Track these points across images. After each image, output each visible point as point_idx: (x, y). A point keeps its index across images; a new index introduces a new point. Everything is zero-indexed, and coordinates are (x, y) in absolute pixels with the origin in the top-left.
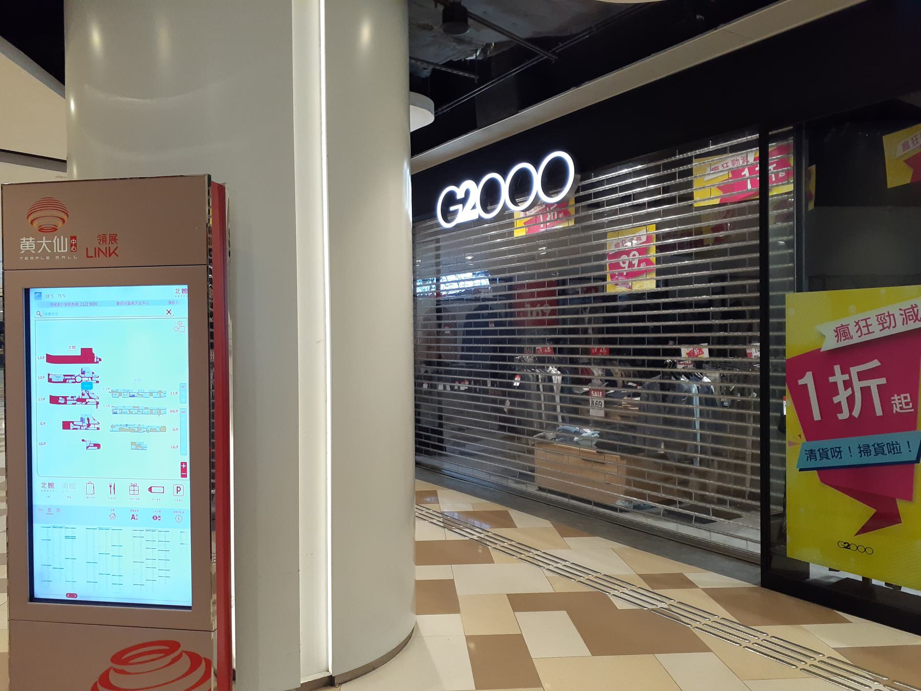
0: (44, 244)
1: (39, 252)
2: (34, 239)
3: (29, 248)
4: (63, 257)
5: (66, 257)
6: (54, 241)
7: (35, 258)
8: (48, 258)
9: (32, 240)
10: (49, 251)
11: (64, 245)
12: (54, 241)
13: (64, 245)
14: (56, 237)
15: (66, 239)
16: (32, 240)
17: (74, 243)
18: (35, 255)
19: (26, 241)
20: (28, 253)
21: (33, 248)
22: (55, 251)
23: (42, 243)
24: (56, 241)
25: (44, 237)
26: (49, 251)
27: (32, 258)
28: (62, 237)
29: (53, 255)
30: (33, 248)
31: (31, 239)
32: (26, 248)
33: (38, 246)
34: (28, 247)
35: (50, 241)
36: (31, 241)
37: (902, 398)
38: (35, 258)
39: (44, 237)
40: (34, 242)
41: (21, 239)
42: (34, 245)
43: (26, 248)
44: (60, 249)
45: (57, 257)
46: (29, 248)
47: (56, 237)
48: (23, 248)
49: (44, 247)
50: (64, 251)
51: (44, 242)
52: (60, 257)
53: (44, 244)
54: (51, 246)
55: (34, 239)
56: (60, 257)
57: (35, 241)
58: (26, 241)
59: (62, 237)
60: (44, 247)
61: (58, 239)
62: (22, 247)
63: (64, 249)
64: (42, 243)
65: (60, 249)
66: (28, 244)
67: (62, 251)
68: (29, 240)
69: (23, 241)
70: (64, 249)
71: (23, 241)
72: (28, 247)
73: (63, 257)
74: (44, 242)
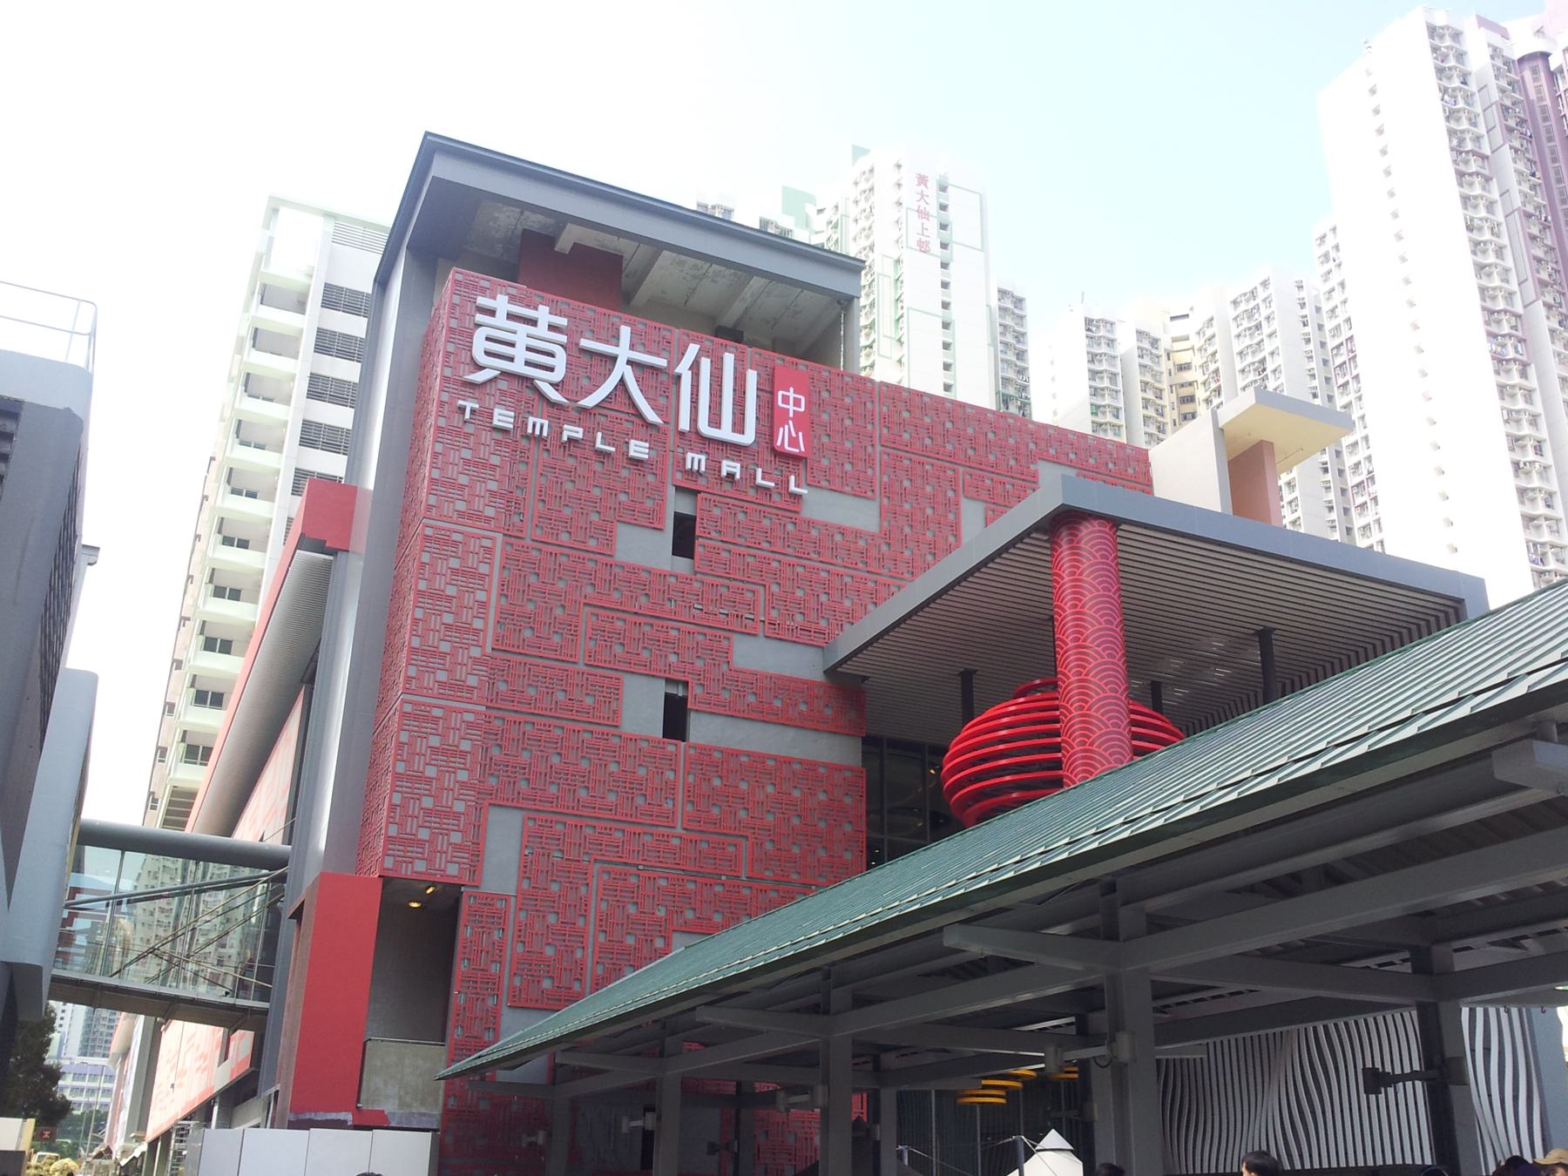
0: (621, 369)
1: (590, 401)
2: (562, 321)
3: (528, 363)
6: (683, 368)
9: (552, 328)
10: (652, 416)
11: (739, 403)
12: (683, 368)
13: (739, 403)
14: (693, 349)
15: (752, 377)
16: (552, 328)
17: (791, 408)
19: (511, 317)
21: (551, 369)
22: (684, 425)
23: (614, 359)
24: (695, 368)
25: (625, 332)
30: (551, 369)
32: (511, 359)
34: (520, 354)
39: (625, 332)
40: (563, 339)
41: (482, 301)
42: (561, 355)
43: (511, 359)
44: (715, 421)
45: (696, 460)
46: (528, 363)
48: (488, 353)
49: (622, 381)
51: (623, 351)
54: (660, 382)
55: (562, 321)
58: (511, 317)
60: (622, 381)
61: (706, 364)
63: (739, 426)
64: (614, 359)
65: (715, 421)
67: (726, 433)
69: (491, 312)
70: (739, 426)
71: (491, 312)
72: (520, 354)
73: (729, 466)
74: (623, 351)
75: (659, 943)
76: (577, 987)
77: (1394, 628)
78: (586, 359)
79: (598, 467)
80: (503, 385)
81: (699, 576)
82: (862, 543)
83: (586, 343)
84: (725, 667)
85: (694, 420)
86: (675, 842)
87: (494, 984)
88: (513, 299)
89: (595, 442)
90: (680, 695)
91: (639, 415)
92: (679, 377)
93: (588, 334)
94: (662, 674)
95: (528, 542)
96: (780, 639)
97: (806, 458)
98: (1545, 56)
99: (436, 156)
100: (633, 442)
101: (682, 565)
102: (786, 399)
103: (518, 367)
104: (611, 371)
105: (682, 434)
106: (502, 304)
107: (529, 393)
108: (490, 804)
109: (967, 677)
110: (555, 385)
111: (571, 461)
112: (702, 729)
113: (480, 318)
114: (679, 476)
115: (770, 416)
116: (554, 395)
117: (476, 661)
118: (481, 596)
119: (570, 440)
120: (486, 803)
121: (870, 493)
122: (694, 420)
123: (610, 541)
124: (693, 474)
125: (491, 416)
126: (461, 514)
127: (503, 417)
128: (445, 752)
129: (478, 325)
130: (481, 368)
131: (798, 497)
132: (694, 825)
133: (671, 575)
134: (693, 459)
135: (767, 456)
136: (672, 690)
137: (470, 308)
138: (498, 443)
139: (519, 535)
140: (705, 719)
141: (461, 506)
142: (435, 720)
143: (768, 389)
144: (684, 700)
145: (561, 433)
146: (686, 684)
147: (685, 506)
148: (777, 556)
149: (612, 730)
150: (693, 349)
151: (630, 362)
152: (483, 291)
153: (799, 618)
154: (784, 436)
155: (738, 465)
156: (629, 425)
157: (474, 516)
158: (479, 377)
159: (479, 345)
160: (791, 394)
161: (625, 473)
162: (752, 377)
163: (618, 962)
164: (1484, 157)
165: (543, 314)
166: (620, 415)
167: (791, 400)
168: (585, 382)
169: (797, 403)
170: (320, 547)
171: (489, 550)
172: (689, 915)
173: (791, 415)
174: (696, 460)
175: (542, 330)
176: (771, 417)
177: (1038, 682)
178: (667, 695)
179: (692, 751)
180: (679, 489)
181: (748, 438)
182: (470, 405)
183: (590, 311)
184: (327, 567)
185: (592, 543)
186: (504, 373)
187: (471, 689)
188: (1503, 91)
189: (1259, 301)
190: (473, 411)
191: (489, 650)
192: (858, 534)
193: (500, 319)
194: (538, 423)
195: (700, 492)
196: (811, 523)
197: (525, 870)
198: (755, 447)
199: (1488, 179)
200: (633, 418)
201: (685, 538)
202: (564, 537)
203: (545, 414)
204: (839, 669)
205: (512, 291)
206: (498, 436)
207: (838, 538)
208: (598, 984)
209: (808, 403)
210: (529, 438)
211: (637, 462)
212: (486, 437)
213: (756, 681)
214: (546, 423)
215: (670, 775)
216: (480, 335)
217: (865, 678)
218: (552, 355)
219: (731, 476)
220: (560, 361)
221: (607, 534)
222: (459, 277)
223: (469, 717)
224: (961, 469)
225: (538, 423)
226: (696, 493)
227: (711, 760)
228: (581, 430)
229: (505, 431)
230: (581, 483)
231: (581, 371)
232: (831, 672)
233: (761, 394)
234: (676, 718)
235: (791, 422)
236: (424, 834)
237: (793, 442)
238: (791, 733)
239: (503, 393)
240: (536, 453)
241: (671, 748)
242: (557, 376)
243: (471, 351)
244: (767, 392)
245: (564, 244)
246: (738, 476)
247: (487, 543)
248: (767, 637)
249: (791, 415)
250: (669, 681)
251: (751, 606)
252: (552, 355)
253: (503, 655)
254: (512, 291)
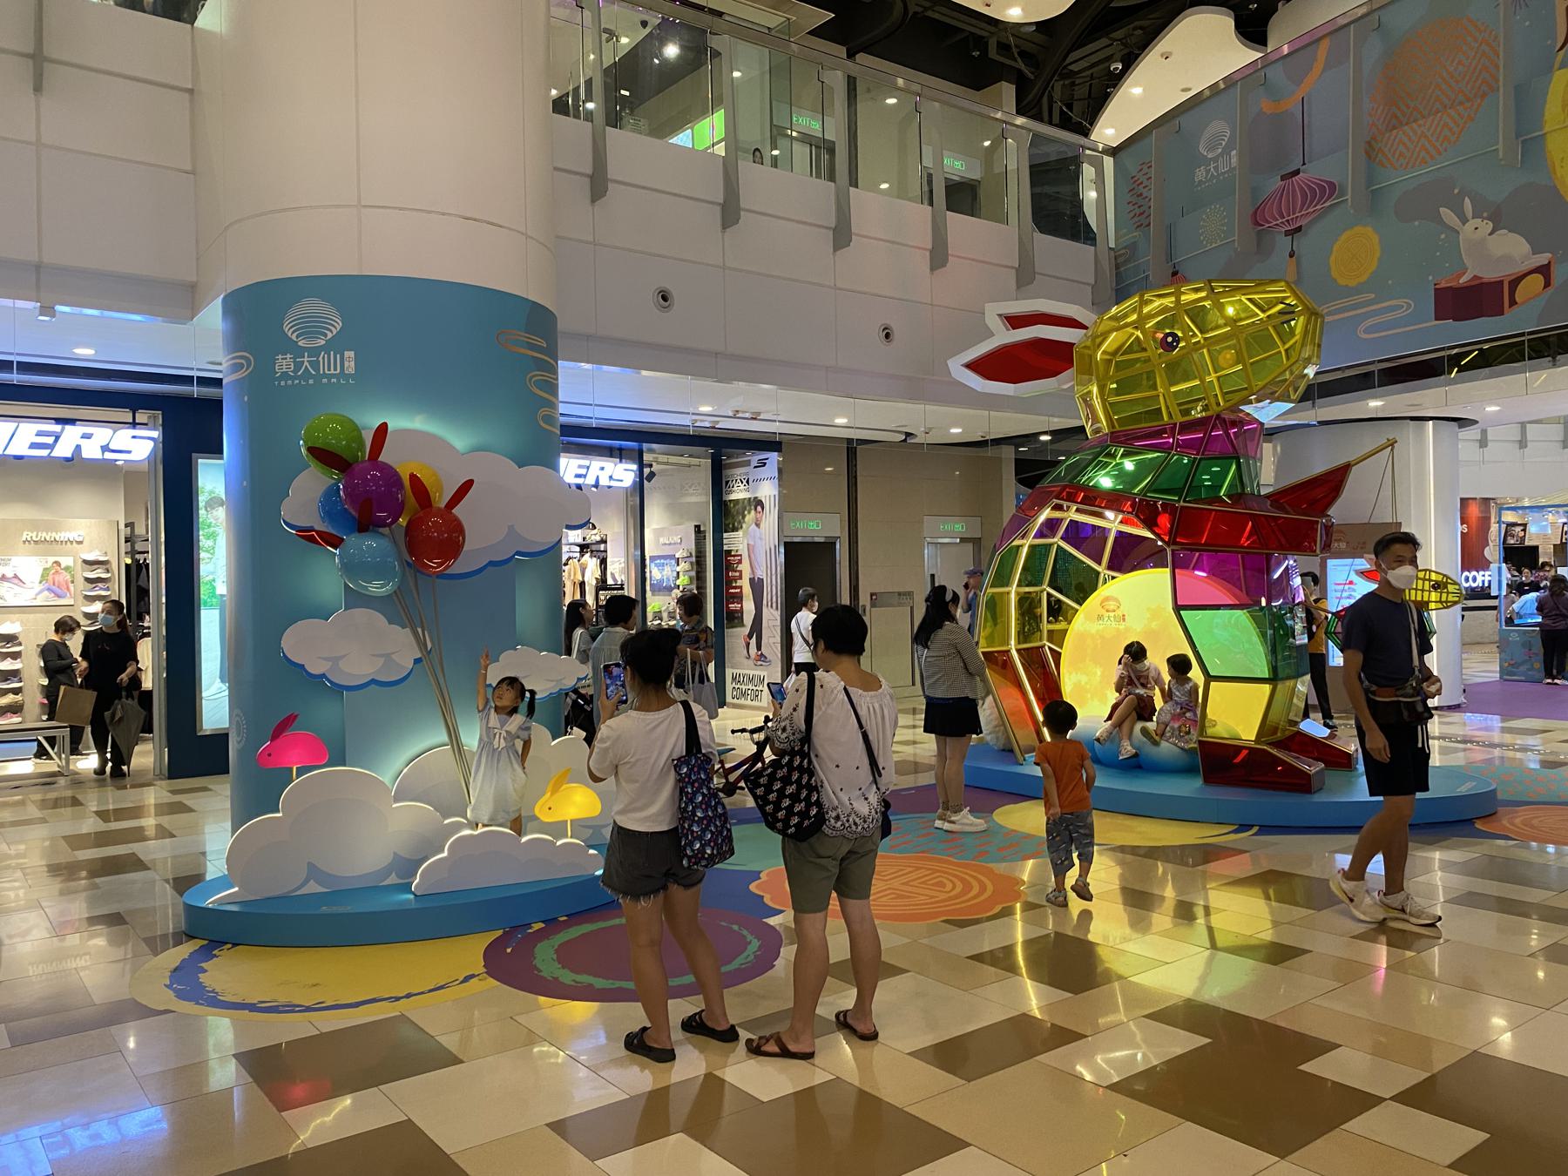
0: (306, 363)
4: (334, 380)
5: (339, 381)
6: (321, 359)
7: (293, 382)
8: (311, 382)
10: (314, 373)
14: (323, 353)
15: (338, 356)
18: (293, 378)
19: (282, 359)
20: (285, 375)
22: (321, 372)
24: (323, 358)
25: (306, 354)
26: (314, 373)
27: (290, 382)
28: (332, 353)
29: (318, 377)
31: (288, 356)
33: (298, 366)
36: (288, 360)
37: (1486, 575)
38: (293, 382)
39: (306, 354)
44: (329, 370)
45: (325, 381)
47: (323, 353)
49: (306, 366)
51: (306, 359)
52: (329, 380)
53: (306, 363)
54: (315, 365)
56: (329, 380)
57: (294, 358)
58: (282, 359)
59: (332, 353)
60: (306, 366)
62: (277, 368)
63: (335, 370)
65: (329, 370)
66: (284, 364)
67: (332, 372)
68: (286, 359)
72: (284, 367)
73: (334, 380)
122: (324, 369)
165: (288, 356)
220: (292, 367)
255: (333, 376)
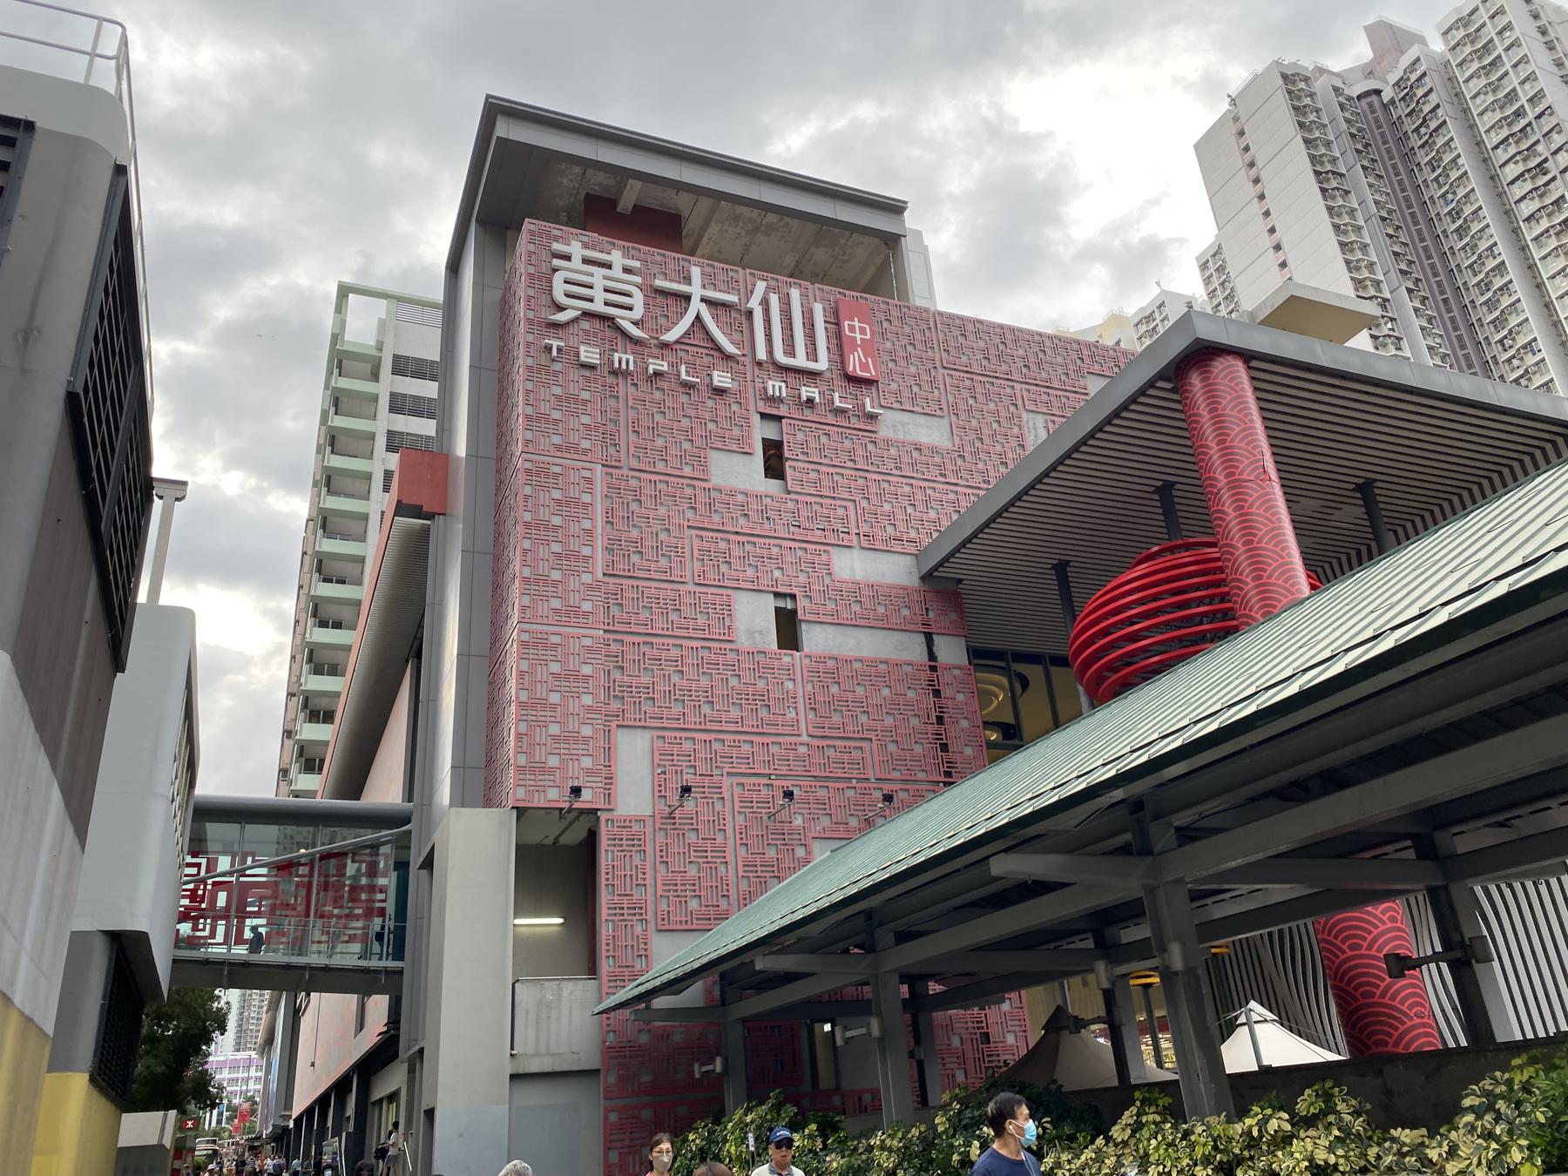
0: (696, 306)
1: (671, 336)
6: (754, 303)
9: (627, 270)
10: (730, 348)
14: (761, 287)
15: (818, 309)
16: (627, 270)
17: (858, 336)
19: (586, 261)
22: (762, 354)
23: (687, 298)
24: (765, 303)
25: (696, 272)
32: (591, 300)
34: (599, 295)
35: (733, 298)
40: (638, 280)
41: (557, 246)
45: (776, 386)
49: (698, 318)
50: (811, 365)
55: (637, 264)
58: (586, 261)
60: (698, 318)
61: (774, 299)
63: (812, 354)
64: (687, 298)
67: (801, 361)
68: (609, 266)
69: (568, 258)
70: (812, 354)
71: (568, 258)
72: (599, 295)
75: (800, 852)
76: (723, 903)
77: (1463, 484)
78: (660, 299)
79: (684, 399)
80: (585, 325)
81: (793, 496)
82: (937, 459)
83: (660, 283)
84: (827, 580)
85: (770, 351)
86: (803, 749)
87: (637, 909)
88: (586, 246)
89: (679, 375)
90: (789, 607)
91: (719, 349)
92: (750, 313)
93: (661, 276)
94: (770, 589)
95: (625, 471)
96: (875, 550)
97: (877, 382)
98: (1378, 92)
99: (499, 118)
100: (715, 373)
101: (773, 485)
102: (852, 329)
103: (598, 307)
104: (686, 310)
105: (759, 364)
106: (576, 249)
107: (609, 333)
108: (618, 726)
109: (1061, 569)
110: (635, 323)
111: (658, 395)
112: (815, 639)
113: (556, 262)
114: (761, 404)
115: (839, 345)
116: (635, 332)
117: (590, 587)
118: (587, 524)
119: (657, 374)
120: (614, 724)
121: (939, 413)
122: (770, 351)
123: (705, 467)
124: (772, 400)
125: (578, 355)
126: (559, 448)
127: (589, 354)
128: (567, 677)
129: (555, 270)
130: (561, 309)
131: (873, 417)
132: (820, 732)
133: (766, 496)
134: (774, 386)
135: (839, 382)
136: (781, 604)
137: (545, 255)
138: (587, 379)
139: (617, 464)
140: (817, 629)
141: (557, 440)
142: (554, 647)
143: (833, 320)
144: (794, 612)
145: (647, 369)
146: (793, 597)
147: (770, 431)
148: (862, 474)
149: (728, 646)
150: (761, 287)
151: (703, 300)
152: (556, 239)
153: (890, 529)
154: (854, 365)
155: (816, 390)
156: (710, 359)
157: (569, 448)
158: (562, 317)
159: (559, 289)
160: (856, 324)
161: (710, 403)
162: (818, 309)
163: (764, 876)
164: (1342, 175)
165: (617, 258)
166: (700, 350)
167: (856, 329)
168: (662, 321)
169: (863, 331)
170: (417, 512)
171: (589, 481)
172: (826, 821)
173: (859, 343)
174: (776, 386)
175: (617, 272)
176: (840, 346)
177: (1156, 549)
178: (777, 609)
179: (807, 661)
180: (764, 416)
181: (822, 364)
182: (555, 344)
183: (656, 254)
184: (426, 530)
185: (687, 471)
186: (587, 314)
187: (586, 614)
188: (1347, 121)
189: (1158, 321)
190: (559, 350)
191: (600, 576)
192: (934, 450)
193: (576, 263)
194: (624, 358)
195: (783, 417)
196: (889, 443)
197: (660, 793)
198: (828, 375)
199: (1347, 192)
200: (712, 352)
201: (774, 463)
202: (660, 466)
203: (629, 351)
204: (935, 574)
205: (585, 239)
206: (587, 373)
207: (916, 454)
208: (746, 899)
209: (872, 332)
210: (615, 373)
211: (720, 392)
212: (574, 374)
213: (857, 590)
214: (631, 358)
215: (789, 685)
216: (558, 278)
217: (959, 581)
218: (628, 295)
219: (810, 401)
220: (638, 300)
221: (700, 461)
222: (532, 227)
223: (587, 642)
224: (1018, 386)
225: (624, 358)
226: (779, 418)
227: (831, 669)
228: (665, 364)
229: (592, 367)
230: (670, 415)
231: (658, 311)
232: (927, 577)
233: (829, 326)
234: (788, 628)
235: (859, 349)
236: (553, 761)
237: (864, 367)
238: (897, 637)
239: (587, 332)
240: (623, 388)
241: (787, 659)
242: (638, 313)
243: (551, 294)
244: (835, 322)
245: (626, 203)
246: (817, 400)
247: (587, 474)
248: (863, 548)
249: (859, 343)
250: (777, 595)
251: (845, 519)
252: (628, 295)
253: (612, 580)
254: (585, 239)
255: (813, 375)
